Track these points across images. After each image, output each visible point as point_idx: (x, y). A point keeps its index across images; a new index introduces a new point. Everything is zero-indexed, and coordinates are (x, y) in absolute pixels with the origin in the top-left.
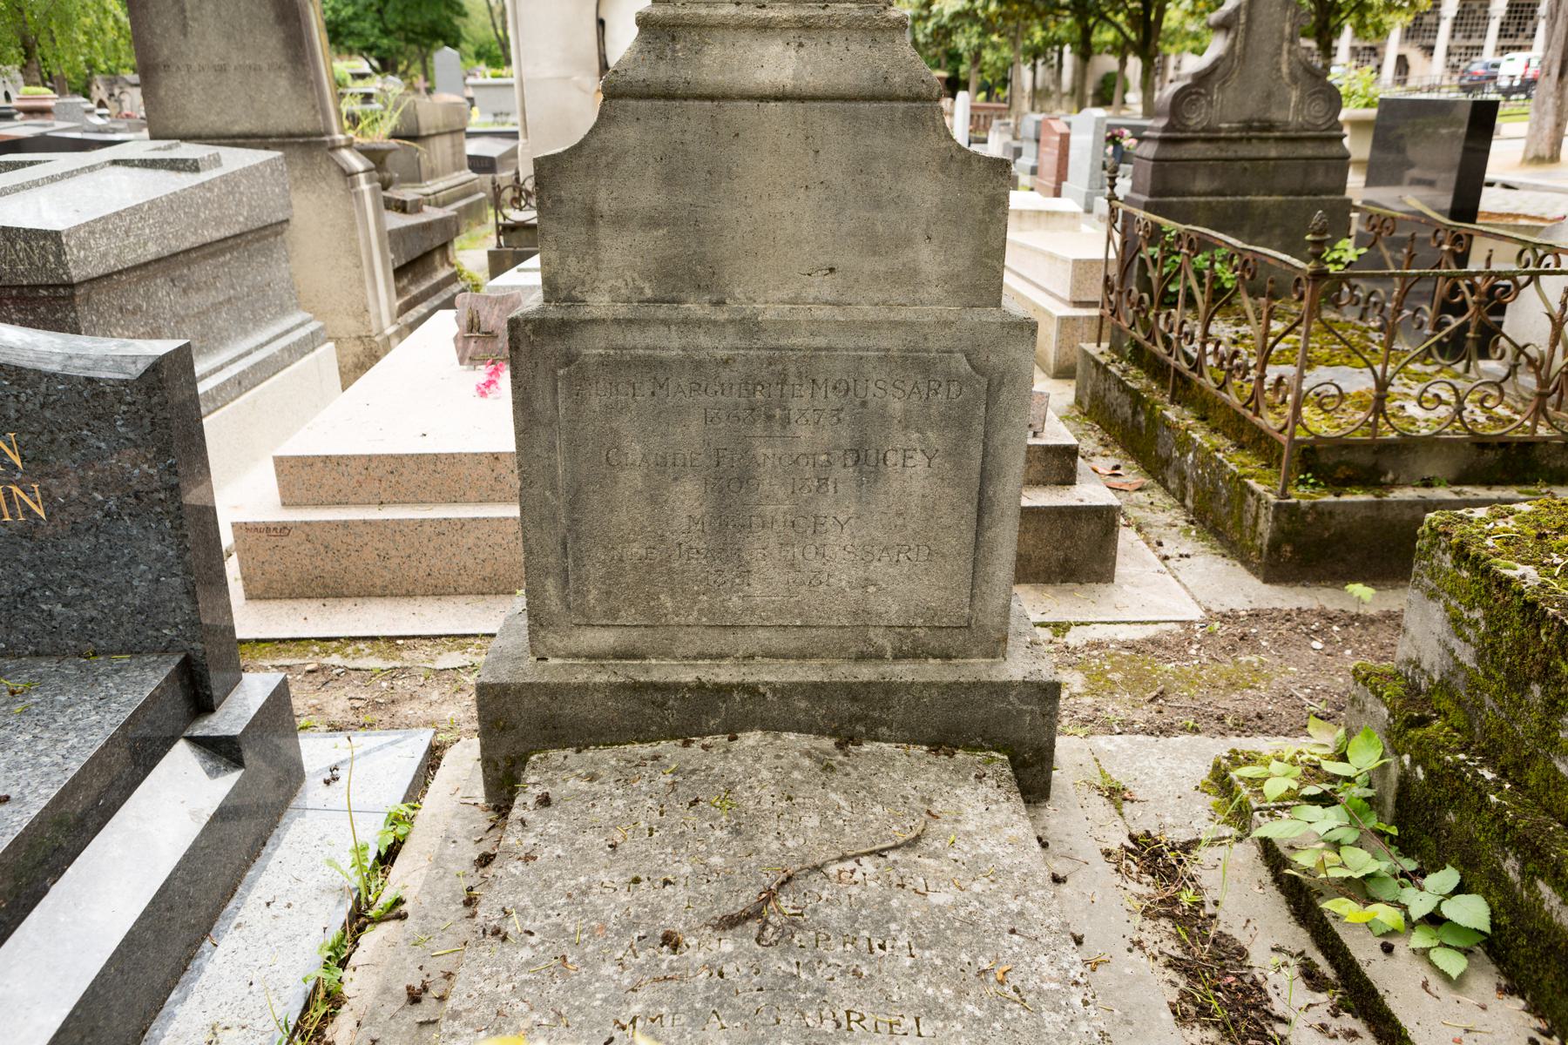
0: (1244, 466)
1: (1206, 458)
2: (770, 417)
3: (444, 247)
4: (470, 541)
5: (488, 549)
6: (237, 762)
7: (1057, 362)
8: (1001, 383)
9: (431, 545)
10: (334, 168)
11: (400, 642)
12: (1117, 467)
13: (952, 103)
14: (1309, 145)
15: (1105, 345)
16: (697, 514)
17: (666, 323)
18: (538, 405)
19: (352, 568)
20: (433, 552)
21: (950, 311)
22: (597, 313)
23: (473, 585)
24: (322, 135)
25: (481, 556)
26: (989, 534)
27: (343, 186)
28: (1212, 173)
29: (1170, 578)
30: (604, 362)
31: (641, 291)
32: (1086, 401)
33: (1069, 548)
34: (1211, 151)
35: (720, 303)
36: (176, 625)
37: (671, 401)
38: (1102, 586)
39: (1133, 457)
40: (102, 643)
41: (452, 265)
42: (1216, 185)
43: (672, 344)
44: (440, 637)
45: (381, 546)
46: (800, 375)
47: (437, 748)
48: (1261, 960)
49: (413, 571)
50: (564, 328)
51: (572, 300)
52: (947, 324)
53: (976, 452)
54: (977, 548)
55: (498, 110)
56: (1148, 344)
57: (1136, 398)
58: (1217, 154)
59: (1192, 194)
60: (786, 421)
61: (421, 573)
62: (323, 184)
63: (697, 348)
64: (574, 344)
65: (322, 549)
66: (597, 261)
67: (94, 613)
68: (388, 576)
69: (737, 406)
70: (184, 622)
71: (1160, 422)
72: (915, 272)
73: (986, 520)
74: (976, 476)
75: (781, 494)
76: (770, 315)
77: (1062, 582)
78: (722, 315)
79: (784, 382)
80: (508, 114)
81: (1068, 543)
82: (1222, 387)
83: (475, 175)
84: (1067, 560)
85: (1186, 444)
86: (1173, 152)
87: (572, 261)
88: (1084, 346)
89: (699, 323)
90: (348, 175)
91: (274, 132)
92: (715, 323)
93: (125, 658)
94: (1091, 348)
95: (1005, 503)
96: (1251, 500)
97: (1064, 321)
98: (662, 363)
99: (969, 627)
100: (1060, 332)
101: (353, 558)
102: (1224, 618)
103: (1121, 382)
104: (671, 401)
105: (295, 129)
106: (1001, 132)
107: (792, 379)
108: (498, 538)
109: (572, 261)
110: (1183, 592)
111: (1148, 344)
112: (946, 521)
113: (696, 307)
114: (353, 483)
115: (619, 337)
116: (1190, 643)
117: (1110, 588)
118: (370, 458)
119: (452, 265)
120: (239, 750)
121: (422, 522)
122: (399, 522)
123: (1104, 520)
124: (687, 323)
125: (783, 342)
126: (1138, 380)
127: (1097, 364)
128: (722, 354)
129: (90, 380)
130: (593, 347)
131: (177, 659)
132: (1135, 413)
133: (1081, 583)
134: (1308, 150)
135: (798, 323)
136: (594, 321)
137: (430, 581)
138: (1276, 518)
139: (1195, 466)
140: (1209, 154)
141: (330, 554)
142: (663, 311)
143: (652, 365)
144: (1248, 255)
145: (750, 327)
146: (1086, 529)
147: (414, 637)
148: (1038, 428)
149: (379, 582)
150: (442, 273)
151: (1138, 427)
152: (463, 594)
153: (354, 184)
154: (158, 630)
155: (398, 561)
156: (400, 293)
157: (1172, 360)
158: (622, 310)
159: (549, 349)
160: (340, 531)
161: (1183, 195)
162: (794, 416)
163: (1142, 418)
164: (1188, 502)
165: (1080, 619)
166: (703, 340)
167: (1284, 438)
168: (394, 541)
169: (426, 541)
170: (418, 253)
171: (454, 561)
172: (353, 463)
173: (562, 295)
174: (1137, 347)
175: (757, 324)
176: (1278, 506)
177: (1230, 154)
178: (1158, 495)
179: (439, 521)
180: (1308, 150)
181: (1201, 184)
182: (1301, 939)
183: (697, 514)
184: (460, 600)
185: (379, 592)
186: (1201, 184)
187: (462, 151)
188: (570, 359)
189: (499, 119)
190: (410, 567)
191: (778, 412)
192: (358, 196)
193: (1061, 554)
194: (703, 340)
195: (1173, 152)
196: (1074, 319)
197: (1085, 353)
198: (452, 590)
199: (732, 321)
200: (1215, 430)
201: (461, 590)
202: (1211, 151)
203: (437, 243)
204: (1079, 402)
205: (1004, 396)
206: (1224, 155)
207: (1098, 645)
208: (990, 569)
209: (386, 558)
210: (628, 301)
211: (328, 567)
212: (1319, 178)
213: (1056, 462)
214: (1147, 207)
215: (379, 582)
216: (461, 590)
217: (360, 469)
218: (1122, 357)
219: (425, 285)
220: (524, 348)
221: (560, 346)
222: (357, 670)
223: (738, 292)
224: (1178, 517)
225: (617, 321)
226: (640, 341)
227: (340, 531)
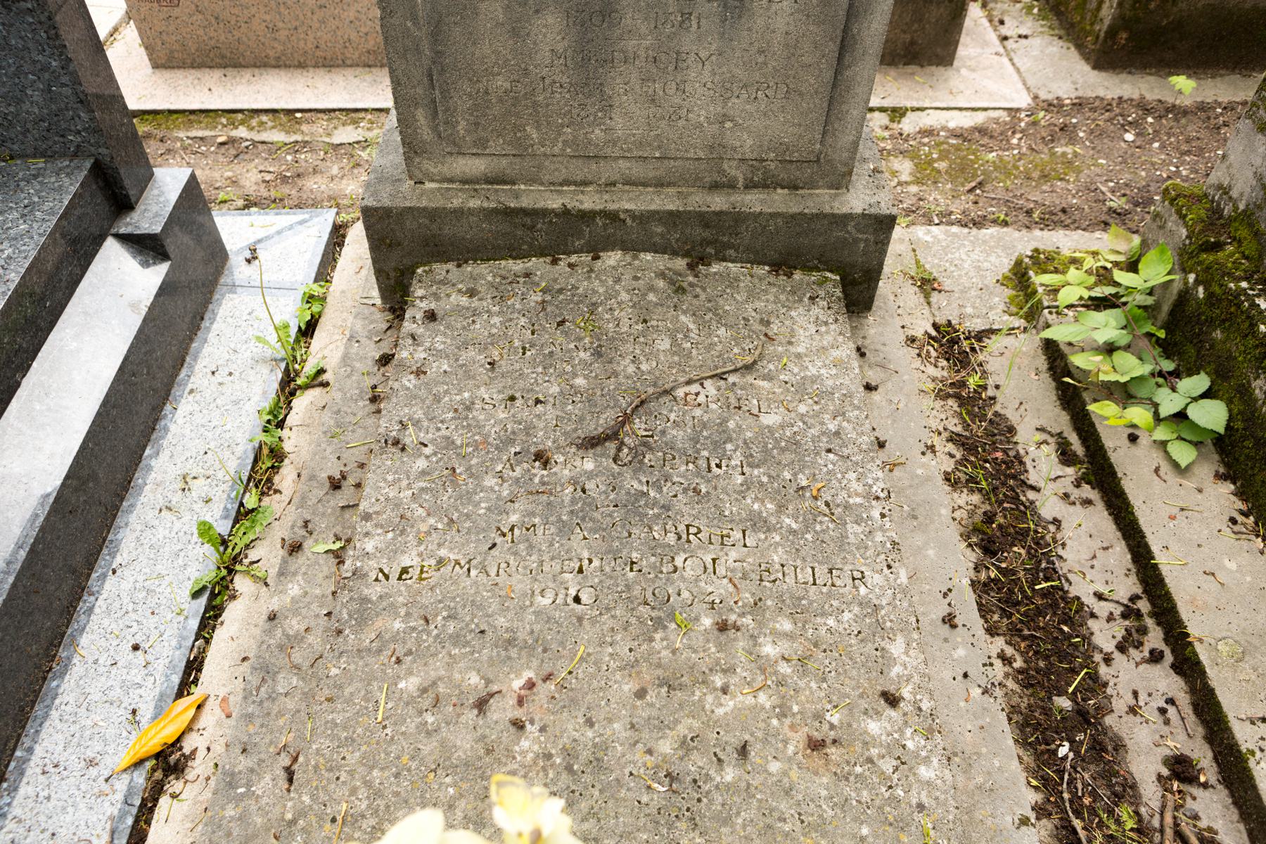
5: (369, 23)
6: (164, 256)
9: (315, 18)
11: (298, 115)
16: (560, 48)
19: (245, 39)
20: (317, 25)
23: (360, 58)
26: (848, 73)
33: (916, 31)
36: (79, 132)
38: (941, 69)
40: (15, 147)
44: (334, 110)
45: (268, 17)
47: (340, 226)
49: (302, 44)
54: (834, 86)
61: (310, 45)
65: (213, 20)
68: (280, 48)
70: (84, 129)
73: (847, 59)
74: (842, 13)
75: (643, 30)
77: (905, 64)
84: (912, 43)
93: (41, 163)
95: (868, 42)
99: (818, 161)
112: (807, 59)
116: (1014, 133)
117: (949, 72)
120: (163, 246)
131: (88, 164)
133: (922, 66)
137: (319, 53)
141: (221, 25)
147: (310, 110)
152: (351, 66)
154: (63, 136)
155: (286, 33)
165: (916, 104)
168: (280, 14)
169: (309, 14)
171: (339, 33)
182: (1061, 421)
183: (560, 48)
184: (349, 72)
185: (273, 63)
190: (299, 40)
193: (908, 37)
198: (340, 62)
201: (348, 62)
208: (845, 108)
211: (222, 38)
215: (271, 53)
216: (348, 62)
222: (263, 142)
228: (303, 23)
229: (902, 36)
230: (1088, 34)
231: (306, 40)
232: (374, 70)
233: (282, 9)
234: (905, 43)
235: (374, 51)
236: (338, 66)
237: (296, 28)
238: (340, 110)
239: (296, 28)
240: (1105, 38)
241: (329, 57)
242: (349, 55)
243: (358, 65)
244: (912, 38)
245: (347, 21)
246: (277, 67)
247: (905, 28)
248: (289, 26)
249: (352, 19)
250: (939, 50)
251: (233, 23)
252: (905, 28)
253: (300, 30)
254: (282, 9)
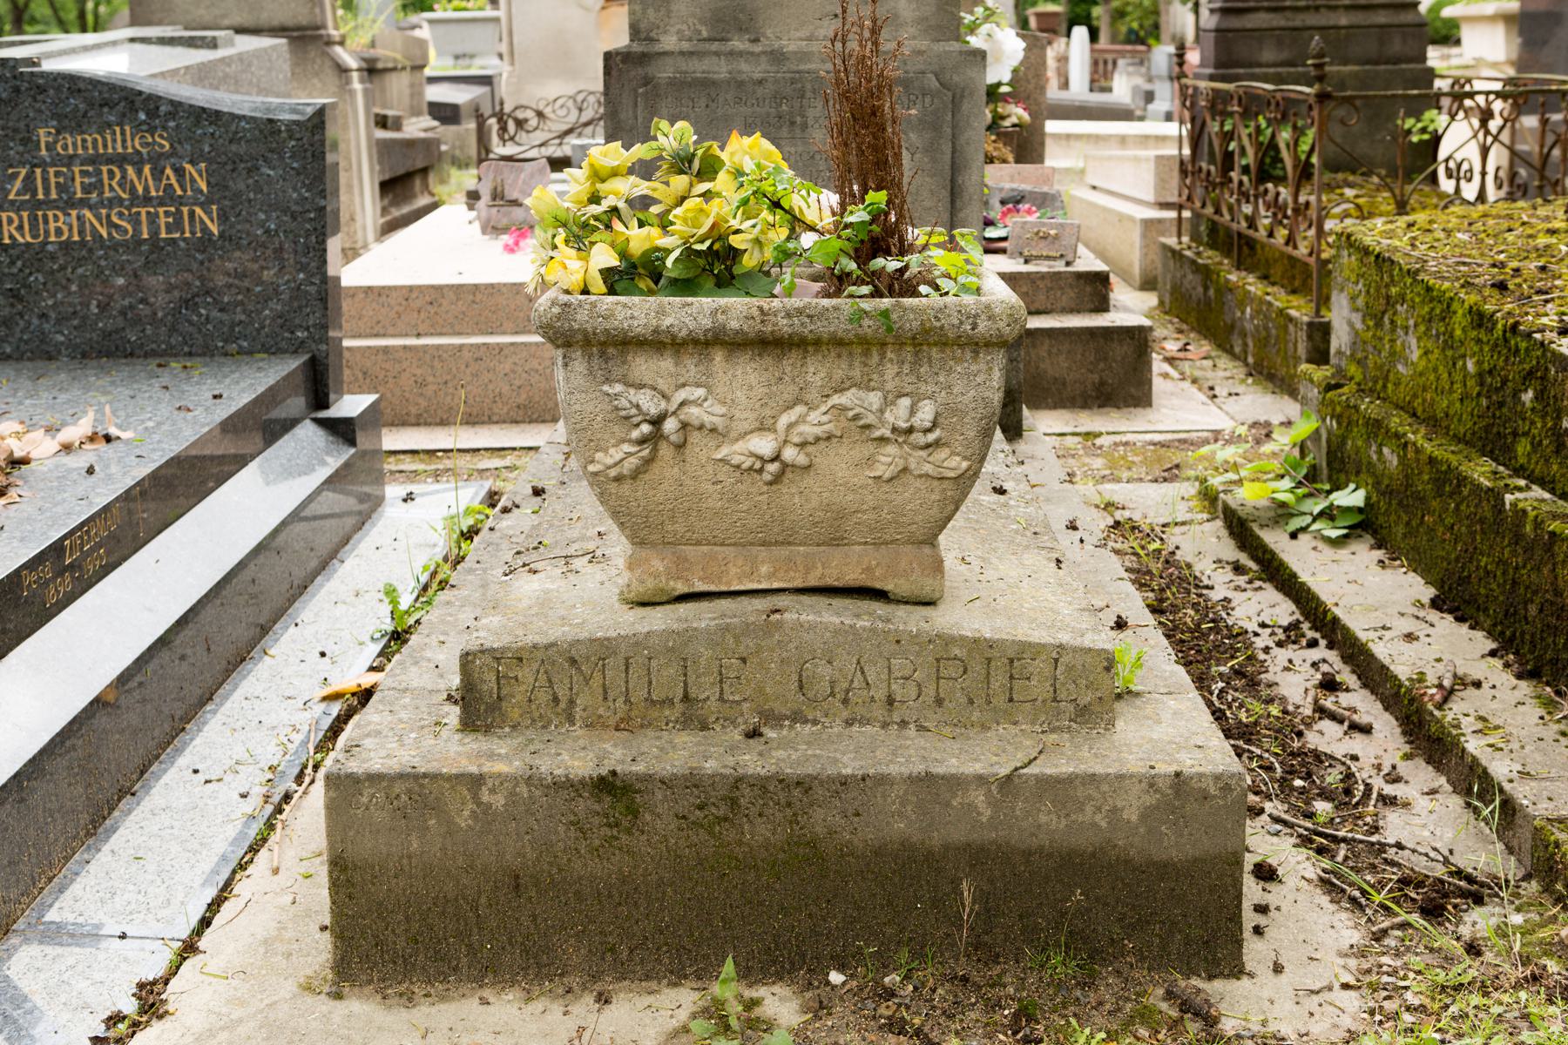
0: (1288, 301)
1: (1263, 307)
2: (793, 123)
3: (424, 171)
4: (507, 366)
5: (524, 375)
6: (352, 442)
7: (1144, 272)
8: (962, 96)
9: (468, 371)
10: (328, 63)
11: (440, 454)
12: (1188, 344)
13: (1068, 44)
15: (1185, 239)
17: (717, 54)
18: (623, 116)
19: (389, 395)
20: (469, 379)
21: (923, 44)
22: (667, 48)
23: (508, 413)
24: (318, 28)
25: (517, 383)
27: (337, 82)
28: (1280, 43)
30: (672, 82)
31: (700, 32)
32: (1167, 300)
33: (1103, 371)
34: (1277, 20)
35: (756, 40)
36: (307, 329)
37: (720, 112)
38: (1139, 411)
39: (1206, 338)
40: (245, 344)
41: (433, 195)
42: (1285, 55)
43: (721, 70)
44: (479, 450)
45: (419, 372)
46: (814, 91)
47: (496, 493)
48: (1204, 568)
49: (449, 398)
50: (644, 58)
51: (651, 40)
52: (920, 53)
53: (947, 148)
55: (459, 51)
56: (1216, 218)
57: (1206, 273)
58: (1283, 23)
59: (1260, 65)
60: (804, 126)
62: (315, 81)
63: (740, 72)
64: (651, 70)
65: (360, 375)
66: (669, 11)
67: (243, 317)
68: (424, 403)
69: (768, 115)
70: (315, 325)
71: (1229, 289)
72: (896, 16)
73: (958, 204)
74: (947, 168)
76: (792, 47)
77: (1099, 407)
78: (757, 48)
79: (803, 97)
80: (472, 56)
81: (1102, 365)
82: (1271, 235)
83: (436, 123)
84: (1102, 383)
85: (1247, 298)
86: (1236, 22)
87: (651, 12)
88: (1163, 240)
89: (741, 54)
90: (343, 70)
91: (266, 26)
92: (752, 54)
93: (265, 356)
94: (1172, 241)
95: (971, 190)
96: (1291, 328)
97: (1148, 224)
98: (714, 83)
100: (1144, 236)
101: (390, 385)
102: (1255, 425)
103: (1193, 262)
104: (720, 112)
105: (290, 22)
106: (1129, 74)
107: (808, 94)
108: (534, 364)
109: (651, 12)
111: (1216, 218)
112: (927, 204)
113: (738, 44)
114: (392, 314)
115: (683, 64)
117: (1148, 410)
118: (411, 289)
119: (433, 195)
120: (354, 431)
121: (461, 346)
122: (438, 347)
123: (1137, 340)
124: (731, 54)
125: (802, 67)
126: (1209, 257)
127: (1173, 251)
128: (757, 76)
130: (664, 72)
131: (306, 357)
132: (1206, 288)
133: (1119, 408)
134: (1381, 18)
135: (812, 53)
136: (665, 53)
138: (1310, 337)
139: (1252, 318)
140: (1275, 24)
141: (368, 381)
142: (715, 46)
143: (707, 85)
144: (1279, 95)
145: (777, 57)
146: (1120, 350)
148: (1070, 258)
149: (414, 410)
150: (423, 201)
151: (1208, 302)
152: (497, 422)
153: (348, 82)
154: (292, 333)
155: (435, 387)
156: (384, 211)
157: (1234, 226)
158: (686, 46)
159: (633, 73)
160: (380, 356)
161: (1251, 65)
162: (810, 122)
163: (1211, 292)
164: (1250, 360)
165: (1111, 430)
166: (744, 67)
167: (1312, 261)
168: (432, 367)
169: (463, 367)
170: (401, 171)
171: (491, 387)
172: (394, 294)
173: (643, 36)
174: (1214, 228)
175: (783, 54)
176: (1310, 324)
177: (1298, 23)
178: (1224, 362)
179: (478, 346)
180: (1381, 18)
181: (1268, 55)
185: (413, 421)
186: (1268, 55)
187: (421, 94)
188: (647, 81)
189: (460, 62)
190: (446, 394)
191: (798, 119)
192: (352, 93)
193: (1096, 378)
194: (744, 67)
195: (1236, 22)
196: (1160, 221)
197: (1165, 247)
198: (486, 418)
199: (764, 53)
200: (1273, 284)
201: (495, 418)
202: (1277, 20)
203: (420, 164)
204: (1161, 303)
205: (965, 107)
206: (1291, 24)
207: (1126, 444)
209: (422, 384)
210: (690, 40)
212: (1396, 46)
213: (1088, 289)
214: (1212, 78)
215: (414, 410)
216: (495, 418)
217: (401, 300)
218: (1200, 243)
219: (406, 209)
220: (614, 73)
221: (640, 71)
222: (401, 472)
223: (769, 33)
224: (1240, 372)
225: (682, 53)
226: (698, 67)
227: (380, 356)
228: (455, 376)
229: (1090, 375)
231: (453, 395)
232: (522, 426)
233: (436, 362)
234: (1094, 383)
235: (525, 406)
236: (483, 423)
237: (446, 383)
238: (486, 449)
239: (446, 383)
241: (475, 413)
242: (496, 411)
243: (504, 422)
244: (1101, 378)
245: (501, 375)
246: (418, 424)
247: (1091, 367)
248: (439, 380)
249: (507, 371)
250: (1133, 390)
251: (381, 377)
252: (1091, 367)
253: (450, 385)
254: (436, 362)
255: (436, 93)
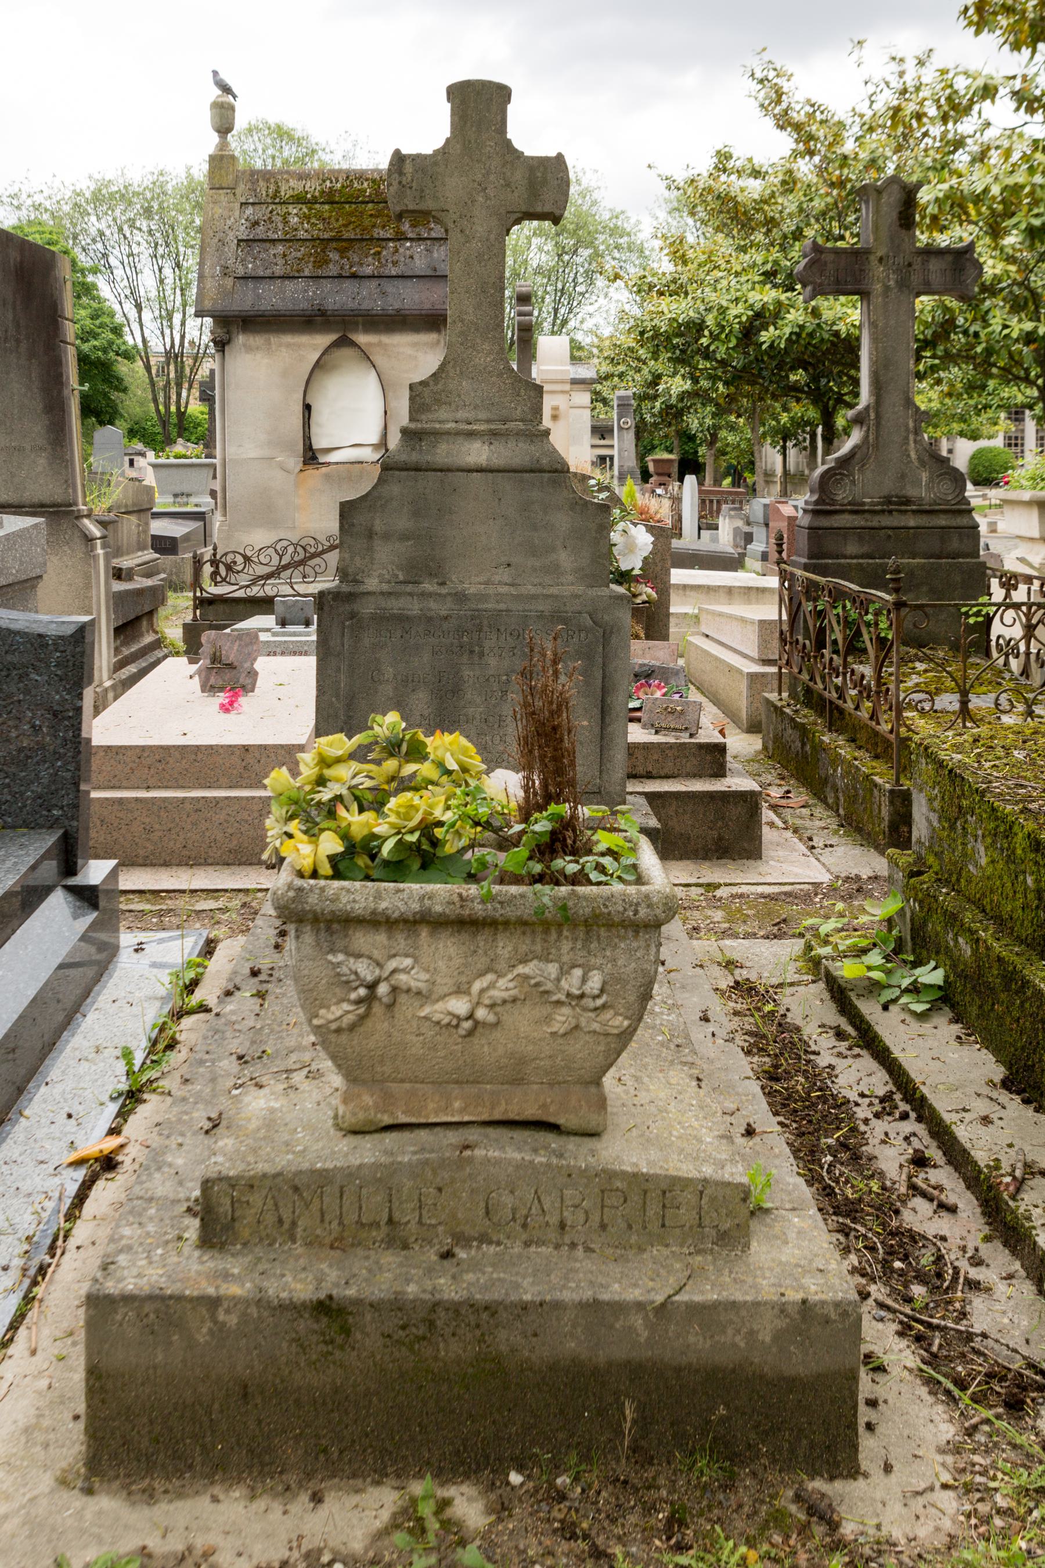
0: (873, 768)
1: (852, 770)
2: (472, 652)
3: (151, 613)
4: (222, 817)
7: (750, 716)
8: (611, 632)
9: (189, 820)
10: (77, 534)
12: (788, 792)
13: (680, 487)
14: (942, 516)
15: (785, 695)
16: (426, 713)
17: (411, 594)
18: (332, 644)
21: (579, 589)
22: (371, 589)
24: (70, 505)
25: (230, 831)
26: (610, 729)
27: (84, 549)
28: (861, 538)
29: (813, 859)
30: (374, 617)
31: (397, 576)
32: (770, 746)
34: (858, 521)
35: (443, 584)
36: (62, 808)
37: (412, 642)
38: (751, 862)
39: (804, 786)
41: (156, 633)
42: (865, 549)
43: (414, 608)
45: (147, 820)
46: (490, 626)
47: (212, 941)
48: (810, 1030)
49: (172, 843)
50: (350, 597)
51: (356, 581)
53: (598, 674)
54: (602, 738)
55: (178, 490)
56: (811, 684)
57: (803, 730)
58: (863, 523)
59: (845, 557)
60: (482, 654)
61: (178, 845)
62: (66, 548)
63: (430, 609)
64: (357, 606)
66: (372, 559)
67: (9, 798)
69: (452, 644)
71: (820, 748)
72: (558, 566)
73: (607, 720)
74: (599, 690)
75: (478, 700)
76: (472, 590)
78: (444, 591)
79: (480, 631)
80: (189, 495)
81: (720, 823)
82: (857, 708)
83: (157, 556)
84: (721, 838)
85: (837, 760)
86: (825, 522)
87: (357, 559)
88: (766, 695)
89: (430, 595)
90: (89, 539)
91: (28, 502)
92: (440, 595)
93: (25, 830)
94: (773, 697)
96: (876, 792)
97: (753, 677)
98: (408, 618)
99: (599, 793)
100: (750, 687)
101: (123, 831)
102: (847, 879)
103: (793, 719)
104: (412, 642)
105: (47, 500)
106: (731, 517)
107: (485, 629)
108: (245, 815)
109: (357, 559)
110: (820, 866)
111: (811, 684)
113: (428, 586)
114: (127, 770)
115: (383, 603)
116: (816, 895)
117: (759, 862)
118: (143, 748)
119: (156, 633)
121: (185, 798)
122: (165, 800)
123: (750, 801)
124: (423, 595)
125: (480, 606)
126: (807, 716)
127: (776, 707)
128: (444, 613)
129: (40, 636)
130: (367, 608)
131: (61, 832)
132: (803, 745)
134: (942, 521)
135: (488, 595)
136: (369, 593)
137: (185, 852)
138: (891, 802)
139: (843, 777)
140: (856, 524)
142: (409, 588)
143: (402, 619)
144: (862, 596)
145: (461, 597)
146: (736, 811)
147: (174, 891)
148: (693, 731)
149: (141, 852)
150: (148, 639)
151: (805, 756)
153: (93, 548)
155: (160, 834)
156: (117, 650)
157: (826, 694)
158: (385, 587)
159: (341, 609)
160: (116, 807)
161: (837, 558)
162: (486, 652)
163: (808, 748)
164: (842, 812)
166: (432, 605)
167: (892, 737)
170: (132, 617)
172: (129, 753)
173: (350, 578)
174: (808, 691)
175: (464, 595)
176: (891, 792)
177: (875, 524)
178: (819, 811)
179: (198, 799)
180: (942, 521)
181: (852, 548)
182: (832, 1017)
183: (426, 713)
184: (210, 869)
185: (141, 861)
186: (852, 548)
187: (146, 531)
188: (353, 615)
189: (179, 500)
191: (477, 649)
192: (95, 558)
194: (432, 605)
195: (825, 522)
196: (763, 675)
197: (768, 701)
199: (450, 594)
200: (860, 748)
202: (858, 521)
203: (147, 609)
204: (765, 748)
205: (614, 640)
206: (869, 524)
207: (741, 896)
208: (612, 753)
209: (150, 831)
210: (389, 582)
211: (101, 839)
212: (955, 544)
213: (708, 758)
214: (806, 568)
215: (141, 852)
216: (210, 861)
217: (134, 758)
218: (797, 701)
219: (134, 648)
220: (326, 608)
221: (347, 607)
223: (454, 577)
224: (833, 823)
225: (382, 593)
226: (395, 605)
227: (116, 807)
230: (877, 834)
236: (200, 864)
238: (202, 891)
240: (890, 834)
255: (159, 527)
